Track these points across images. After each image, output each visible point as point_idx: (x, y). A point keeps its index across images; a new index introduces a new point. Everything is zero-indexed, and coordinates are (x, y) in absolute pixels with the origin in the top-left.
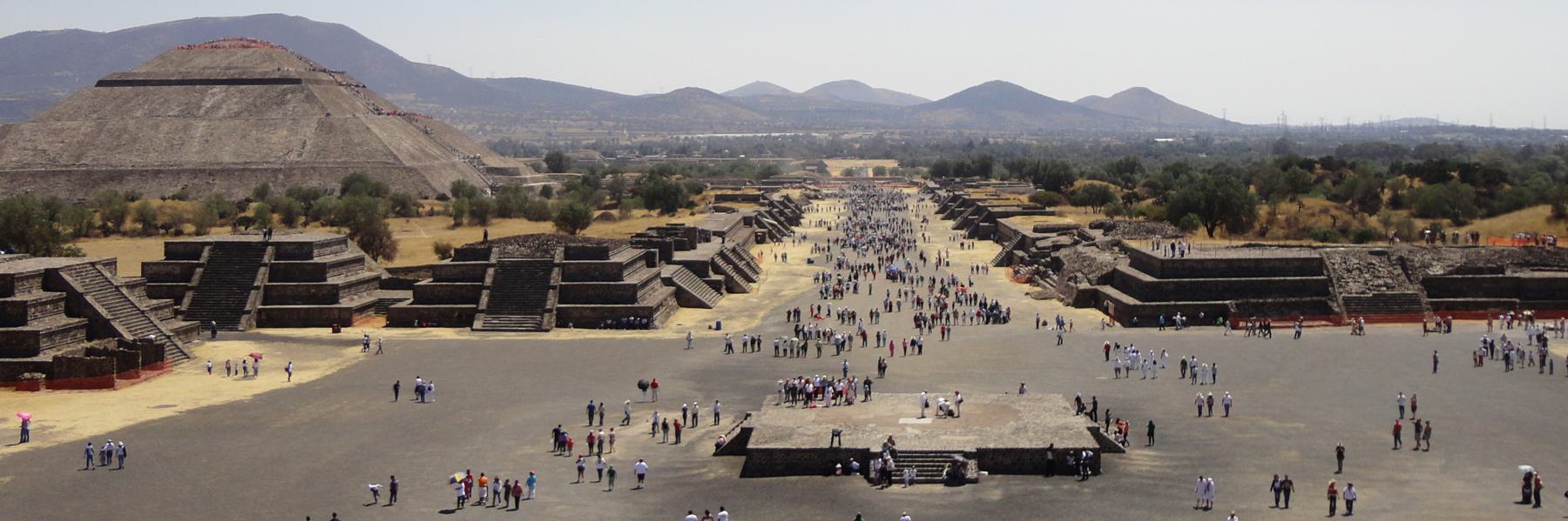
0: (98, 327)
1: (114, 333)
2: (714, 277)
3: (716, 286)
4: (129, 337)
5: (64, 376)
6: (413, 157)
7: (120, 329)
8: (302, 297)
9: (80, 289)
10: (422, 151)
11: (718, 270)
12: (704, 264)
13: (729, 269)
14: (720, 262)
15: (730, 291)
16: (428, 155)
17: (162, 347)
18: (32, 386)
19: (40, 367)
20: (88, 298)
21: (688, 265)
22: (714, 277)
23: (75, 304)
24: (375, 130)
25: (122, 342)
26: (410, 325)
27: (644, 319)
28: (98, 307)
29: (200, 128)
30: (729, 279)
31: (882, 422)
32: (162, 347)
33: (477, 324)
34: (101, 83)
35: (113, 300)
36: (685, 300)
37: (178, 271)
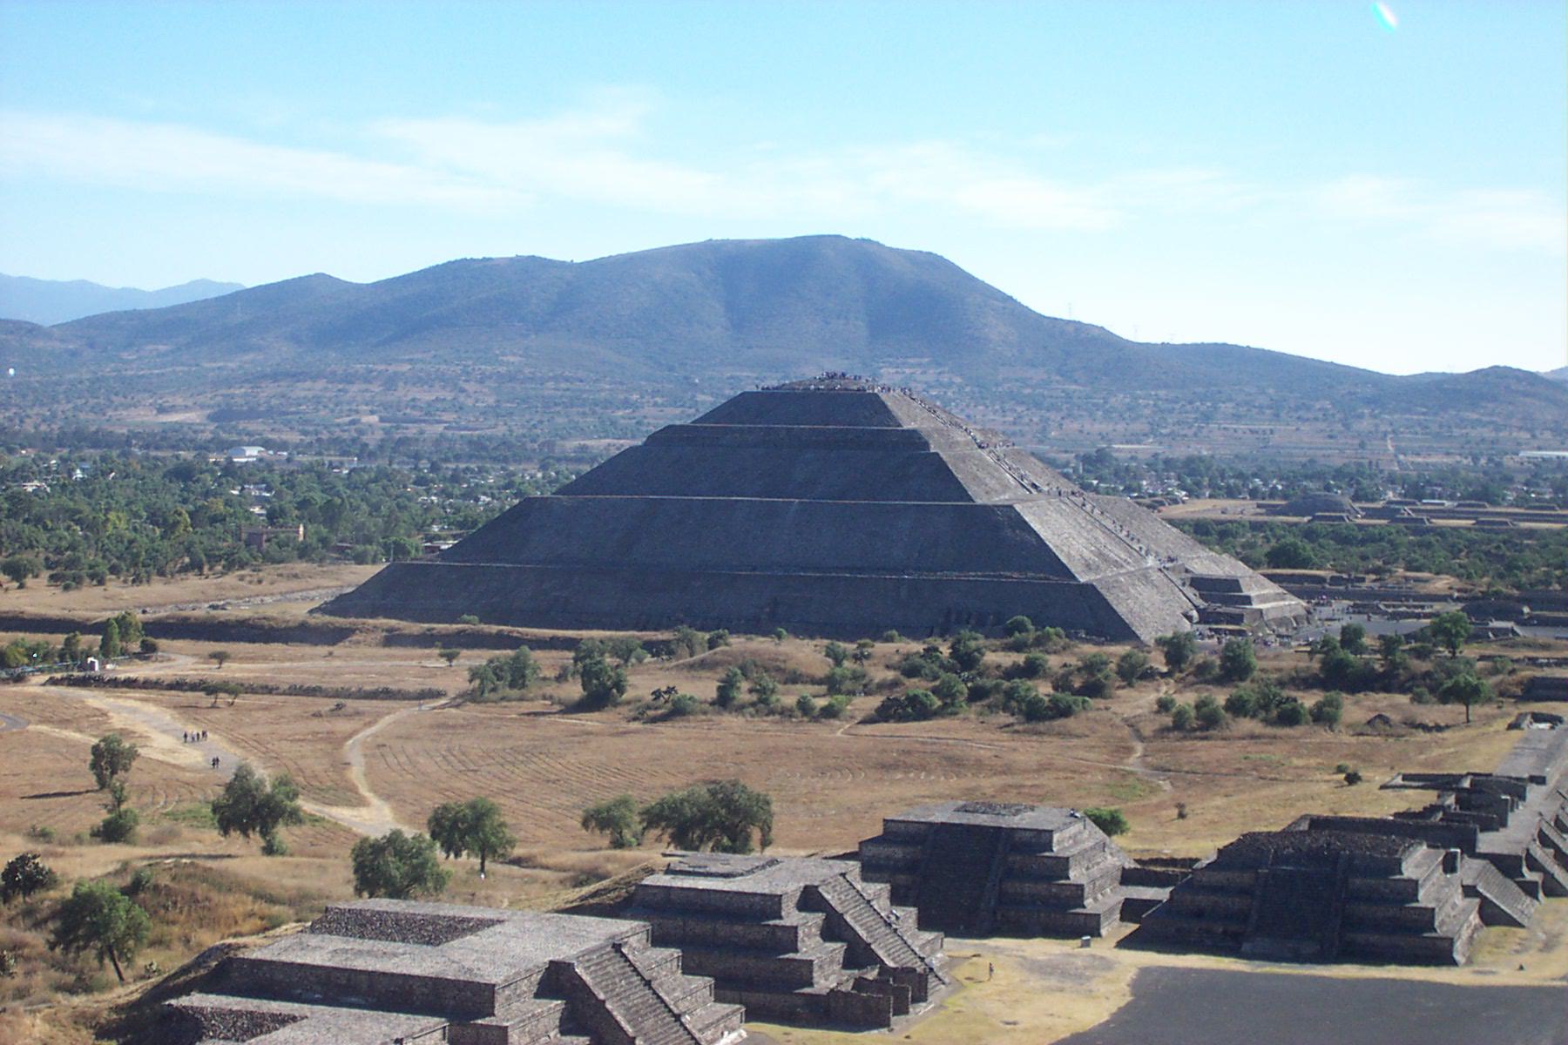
0: (858, 954)
1: (876, 960)
2: (1530, 876)
3: (1530, 890)
4: (891, 964)
6: (1088, 567)
7: (881, 953)
9: (839, 909)
10: (1100, 554)
11: (1534, 865)
14: (1539, 852)
16: (1106, 559)
20: (848, 918)
21: (1496, 860)
22: (1530, 876)
24: (1036, 526)
25: (884, 969)
27: (1441, 955)
28: (858, 929)
30: (1549, 876)
33: (1246, 947)
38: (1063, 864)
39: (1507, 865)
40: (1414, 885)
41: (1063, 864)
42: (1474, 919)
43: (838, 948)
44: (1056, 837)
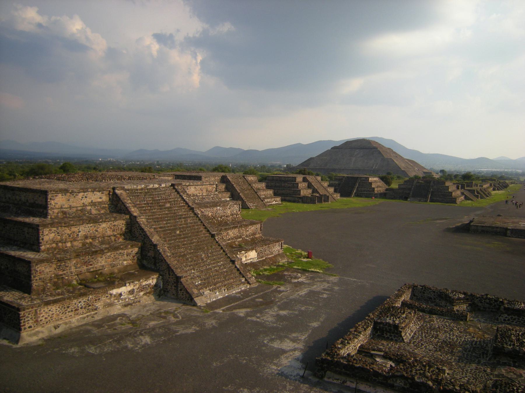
0: (315, 191)
1: (318, 193)
3: (477, 197)
5: (305, 200)
6: (404, 168)
8: (366, 191)
11: (478, 193)
12: (474, 191)
13: (482, 193)
15: (481, 198)
17: (328, 197)
18: (298, 202)
19: (300, 198)
21: (469, 190)
23: (310, 186)
24: (395, 161)
25: (320, 194)
26: (392, 199)
29: (354, 159)
31: (513, 223)
32: (328, 197)
33: (409, 199)
34: (332, 148)
35: (319, 185)
36: (466, 198)
37: (337, 183)
38: (371, 183)
39: (472, 192)
40: (448, 187)
41: (371, 183)
42: (463, 197)
43: (310, 191)
44: (370, 179)
